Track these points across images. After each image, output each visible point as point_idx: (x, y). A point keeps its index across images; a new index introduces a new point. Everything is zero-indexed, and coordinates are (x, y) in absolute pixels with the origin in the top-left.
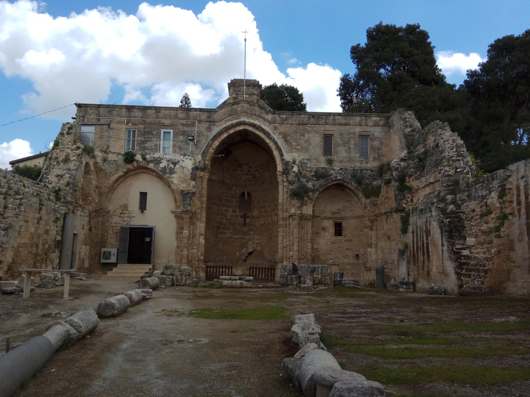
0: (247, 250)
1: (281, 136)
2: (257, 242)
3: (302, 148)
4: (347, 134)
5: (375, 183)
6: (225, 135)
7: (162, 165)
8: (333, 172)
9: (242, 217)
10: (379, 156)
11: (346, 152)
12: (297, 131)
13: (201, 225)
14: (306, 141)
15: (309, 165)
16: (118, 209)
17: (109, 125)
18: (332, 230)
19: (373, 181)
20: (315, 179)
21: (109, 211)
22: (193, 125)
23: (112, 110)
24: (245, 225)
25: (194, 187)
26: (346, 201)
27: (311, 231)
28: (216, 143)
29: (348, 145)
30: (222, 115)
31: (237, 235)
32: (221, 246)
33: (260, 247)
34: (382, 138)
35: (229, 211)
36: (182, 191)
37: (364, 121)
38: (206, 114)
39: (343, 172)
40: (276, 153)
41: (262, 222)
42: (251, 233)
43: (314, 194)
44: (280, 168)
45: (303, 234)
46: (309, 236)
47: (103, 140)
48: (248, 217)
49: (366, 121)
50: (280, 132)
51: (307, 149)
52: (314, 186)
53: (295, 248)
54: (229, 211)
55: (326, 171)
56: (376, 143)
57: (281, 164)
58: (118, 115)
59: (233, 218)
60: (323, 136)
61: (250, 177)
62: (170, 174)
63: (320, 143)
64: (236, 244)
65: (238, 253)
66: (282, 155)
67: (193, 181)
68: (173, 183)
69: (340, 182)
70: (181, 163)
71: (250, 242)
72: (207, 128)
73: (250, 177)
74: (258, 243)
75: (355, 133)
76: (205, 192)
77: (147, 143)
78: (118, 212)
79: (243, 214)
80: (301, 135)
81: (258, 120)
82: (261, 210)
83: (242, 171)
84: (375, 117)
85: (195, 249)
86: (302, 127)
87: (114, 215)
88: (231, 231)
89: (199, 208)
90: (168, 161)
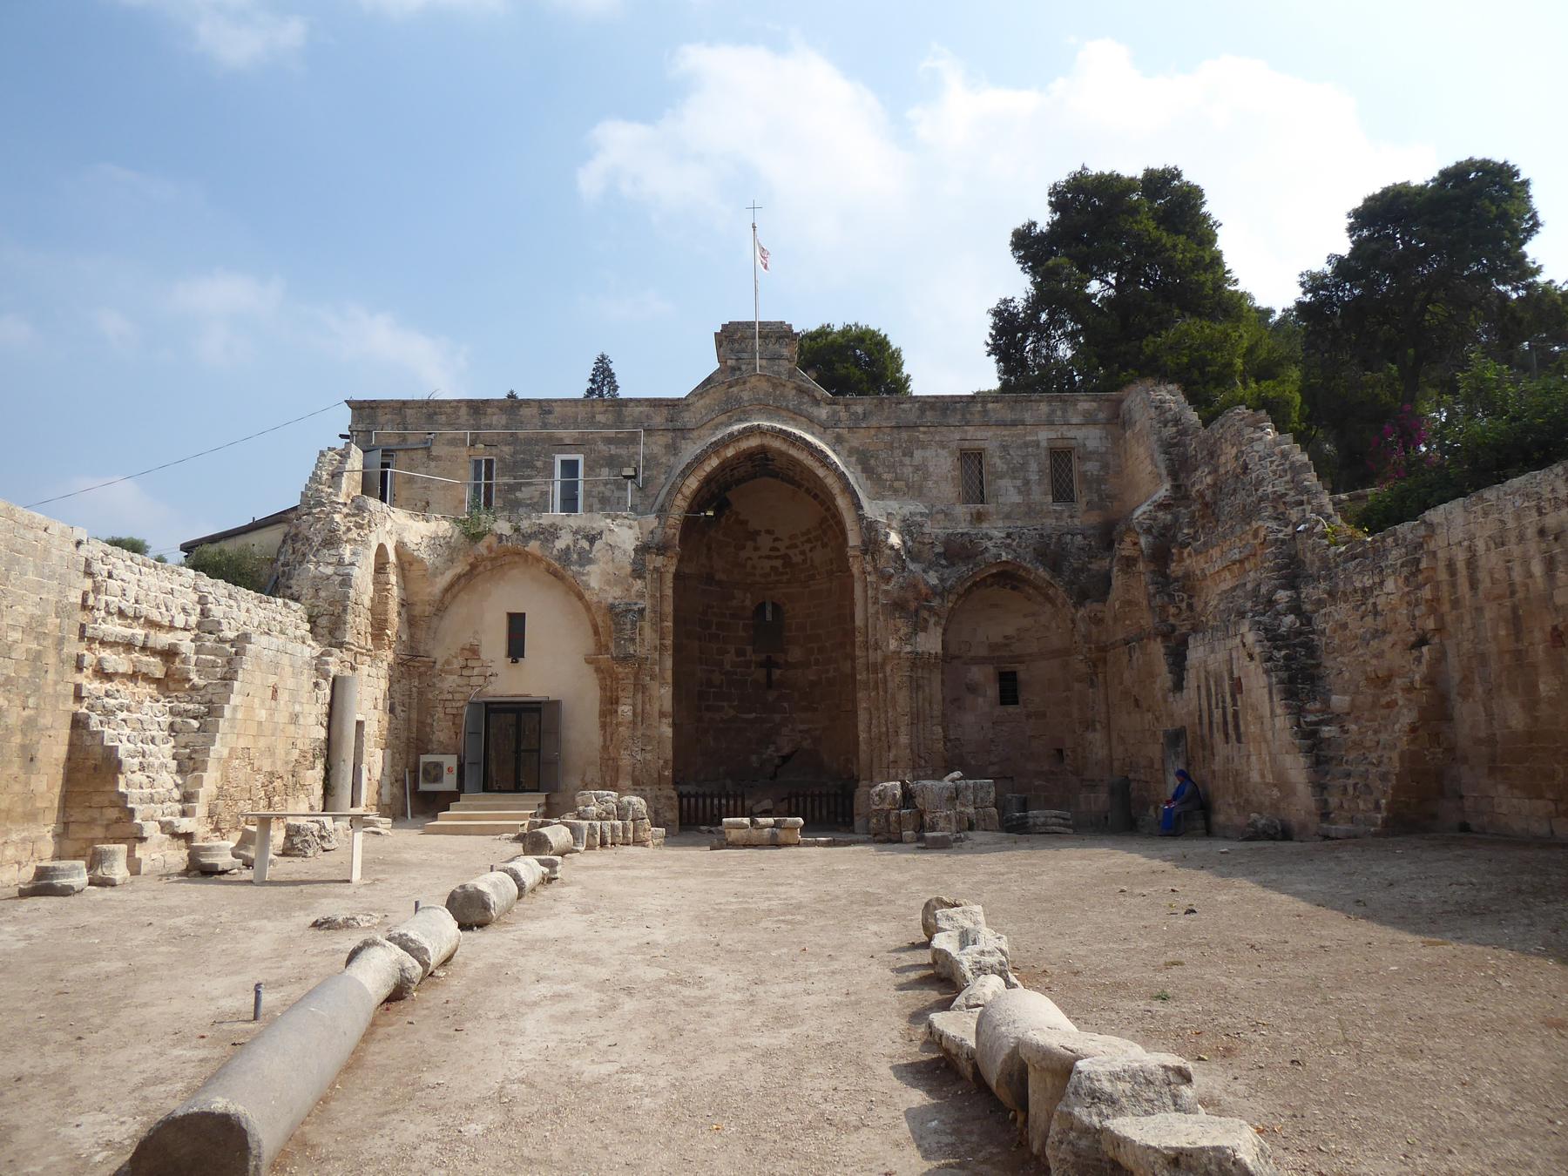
0: (777, 750)
1: (853, 459)
2: (802, 727)
3: (907, 486)
4: (1019, 447)
5: (1094, 567)
6: (715, 462)
7: (560, 544)
8: (989, 544)
9: (761, 665)
10: (1101, 499)
11: (1020, 492)
12: (892, 443)
13: (662, 691)
14: (917, 469)
15: (926, 530)
16: (456, 657)
17: (428, 449)
18: (993, 691)
19: (1091, 563)
20: (943, 562)
21: (435, 662)
22: (633, 439)
23: (435, 414)
24: (769, 684)
25: (641, 595)
26: (1025, 616)
27: (940, 697)
28: (693, 483)
29: (1022, 474)
30: (704, 412)
33: (809, 741)
34: (1106, 453)
36: (612, 607)
37: (1059, 413)
38: (665, 411)
39: (1014, 543)
40: (842, 502)
42: (786, 705)
43: (943, 600)
44: (854, 539)
45: (920, 704)
46: (937, 710)
47: (414, 486)
48: (777, 665)
49: (1065, 411)
50: (851, 448)
51: (920, 488)
52: (942, 580)
53: (904, 739)
54: (728, 652)
55: (971, 541)
56: (1092, 467)
57: (856, 528)
58: (450, 425)
60: (958, 455)
61: (778, 563)
62: (581, 566)
63: (953, 473)
65: (754, 758)
66: (858, 506)
67: (639, 582)
68: (588, 587)
69: (1009, 568)
70: (606, 537)
72: (667, 446)
73: (778, 563)
75: (1037, 444)
76: (668, 608)
77: (520, 490)
78: (457, 664)
79: (763, 656)
80: (904, 455)
81: (794, 419)
83: (756, 549)
84: (1085, 401)
85: (650, 751)
86: (904, 435)
87: (446, 672)
88: (736, 703)
89: (656, 647)
90: (576, 533)
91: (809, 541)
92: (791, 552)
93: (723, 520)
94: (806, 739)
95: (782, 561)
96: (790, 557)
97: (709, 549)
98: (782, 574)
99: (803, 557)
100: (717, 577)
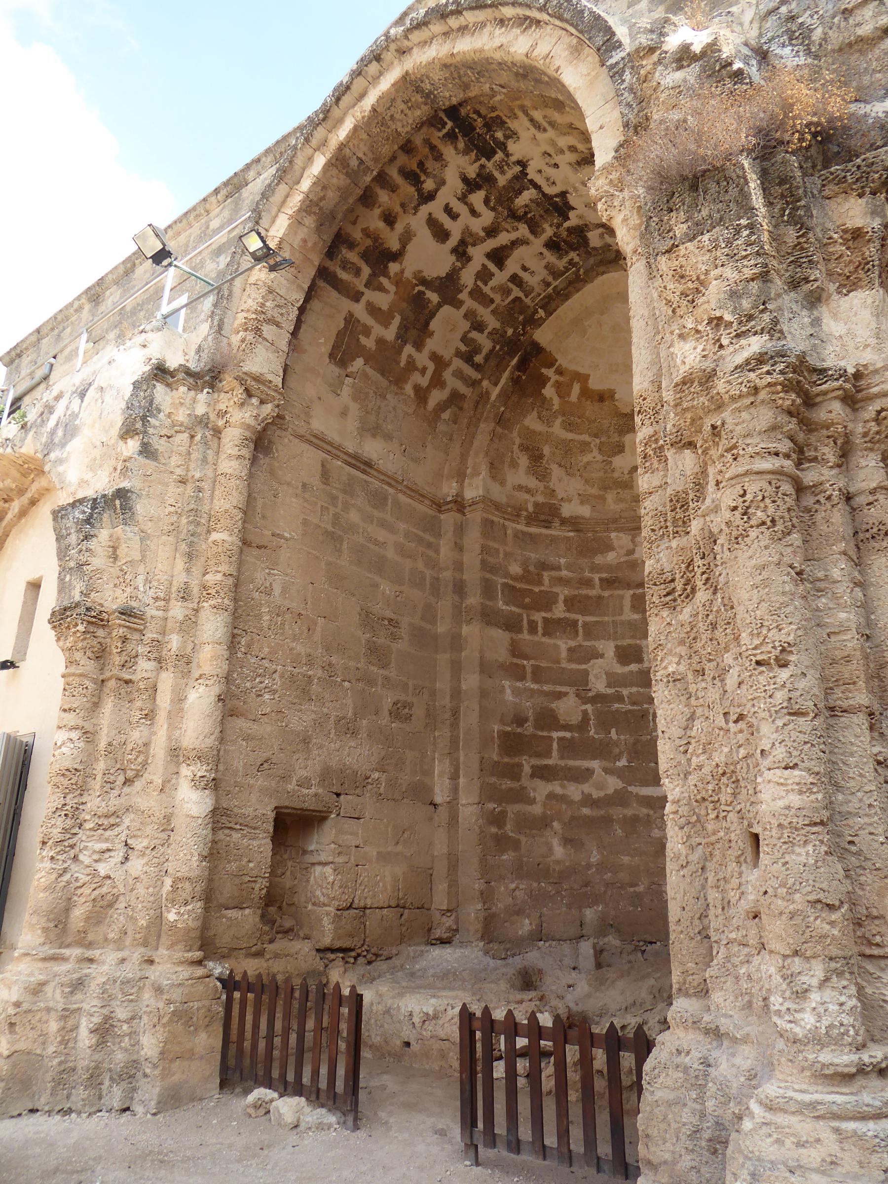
32: (559, 851)
54: (602, 656)
59: (625, 692)
88: (622, 763)
93: (549, 391)
97: (536, 457)
100: (567, 510)
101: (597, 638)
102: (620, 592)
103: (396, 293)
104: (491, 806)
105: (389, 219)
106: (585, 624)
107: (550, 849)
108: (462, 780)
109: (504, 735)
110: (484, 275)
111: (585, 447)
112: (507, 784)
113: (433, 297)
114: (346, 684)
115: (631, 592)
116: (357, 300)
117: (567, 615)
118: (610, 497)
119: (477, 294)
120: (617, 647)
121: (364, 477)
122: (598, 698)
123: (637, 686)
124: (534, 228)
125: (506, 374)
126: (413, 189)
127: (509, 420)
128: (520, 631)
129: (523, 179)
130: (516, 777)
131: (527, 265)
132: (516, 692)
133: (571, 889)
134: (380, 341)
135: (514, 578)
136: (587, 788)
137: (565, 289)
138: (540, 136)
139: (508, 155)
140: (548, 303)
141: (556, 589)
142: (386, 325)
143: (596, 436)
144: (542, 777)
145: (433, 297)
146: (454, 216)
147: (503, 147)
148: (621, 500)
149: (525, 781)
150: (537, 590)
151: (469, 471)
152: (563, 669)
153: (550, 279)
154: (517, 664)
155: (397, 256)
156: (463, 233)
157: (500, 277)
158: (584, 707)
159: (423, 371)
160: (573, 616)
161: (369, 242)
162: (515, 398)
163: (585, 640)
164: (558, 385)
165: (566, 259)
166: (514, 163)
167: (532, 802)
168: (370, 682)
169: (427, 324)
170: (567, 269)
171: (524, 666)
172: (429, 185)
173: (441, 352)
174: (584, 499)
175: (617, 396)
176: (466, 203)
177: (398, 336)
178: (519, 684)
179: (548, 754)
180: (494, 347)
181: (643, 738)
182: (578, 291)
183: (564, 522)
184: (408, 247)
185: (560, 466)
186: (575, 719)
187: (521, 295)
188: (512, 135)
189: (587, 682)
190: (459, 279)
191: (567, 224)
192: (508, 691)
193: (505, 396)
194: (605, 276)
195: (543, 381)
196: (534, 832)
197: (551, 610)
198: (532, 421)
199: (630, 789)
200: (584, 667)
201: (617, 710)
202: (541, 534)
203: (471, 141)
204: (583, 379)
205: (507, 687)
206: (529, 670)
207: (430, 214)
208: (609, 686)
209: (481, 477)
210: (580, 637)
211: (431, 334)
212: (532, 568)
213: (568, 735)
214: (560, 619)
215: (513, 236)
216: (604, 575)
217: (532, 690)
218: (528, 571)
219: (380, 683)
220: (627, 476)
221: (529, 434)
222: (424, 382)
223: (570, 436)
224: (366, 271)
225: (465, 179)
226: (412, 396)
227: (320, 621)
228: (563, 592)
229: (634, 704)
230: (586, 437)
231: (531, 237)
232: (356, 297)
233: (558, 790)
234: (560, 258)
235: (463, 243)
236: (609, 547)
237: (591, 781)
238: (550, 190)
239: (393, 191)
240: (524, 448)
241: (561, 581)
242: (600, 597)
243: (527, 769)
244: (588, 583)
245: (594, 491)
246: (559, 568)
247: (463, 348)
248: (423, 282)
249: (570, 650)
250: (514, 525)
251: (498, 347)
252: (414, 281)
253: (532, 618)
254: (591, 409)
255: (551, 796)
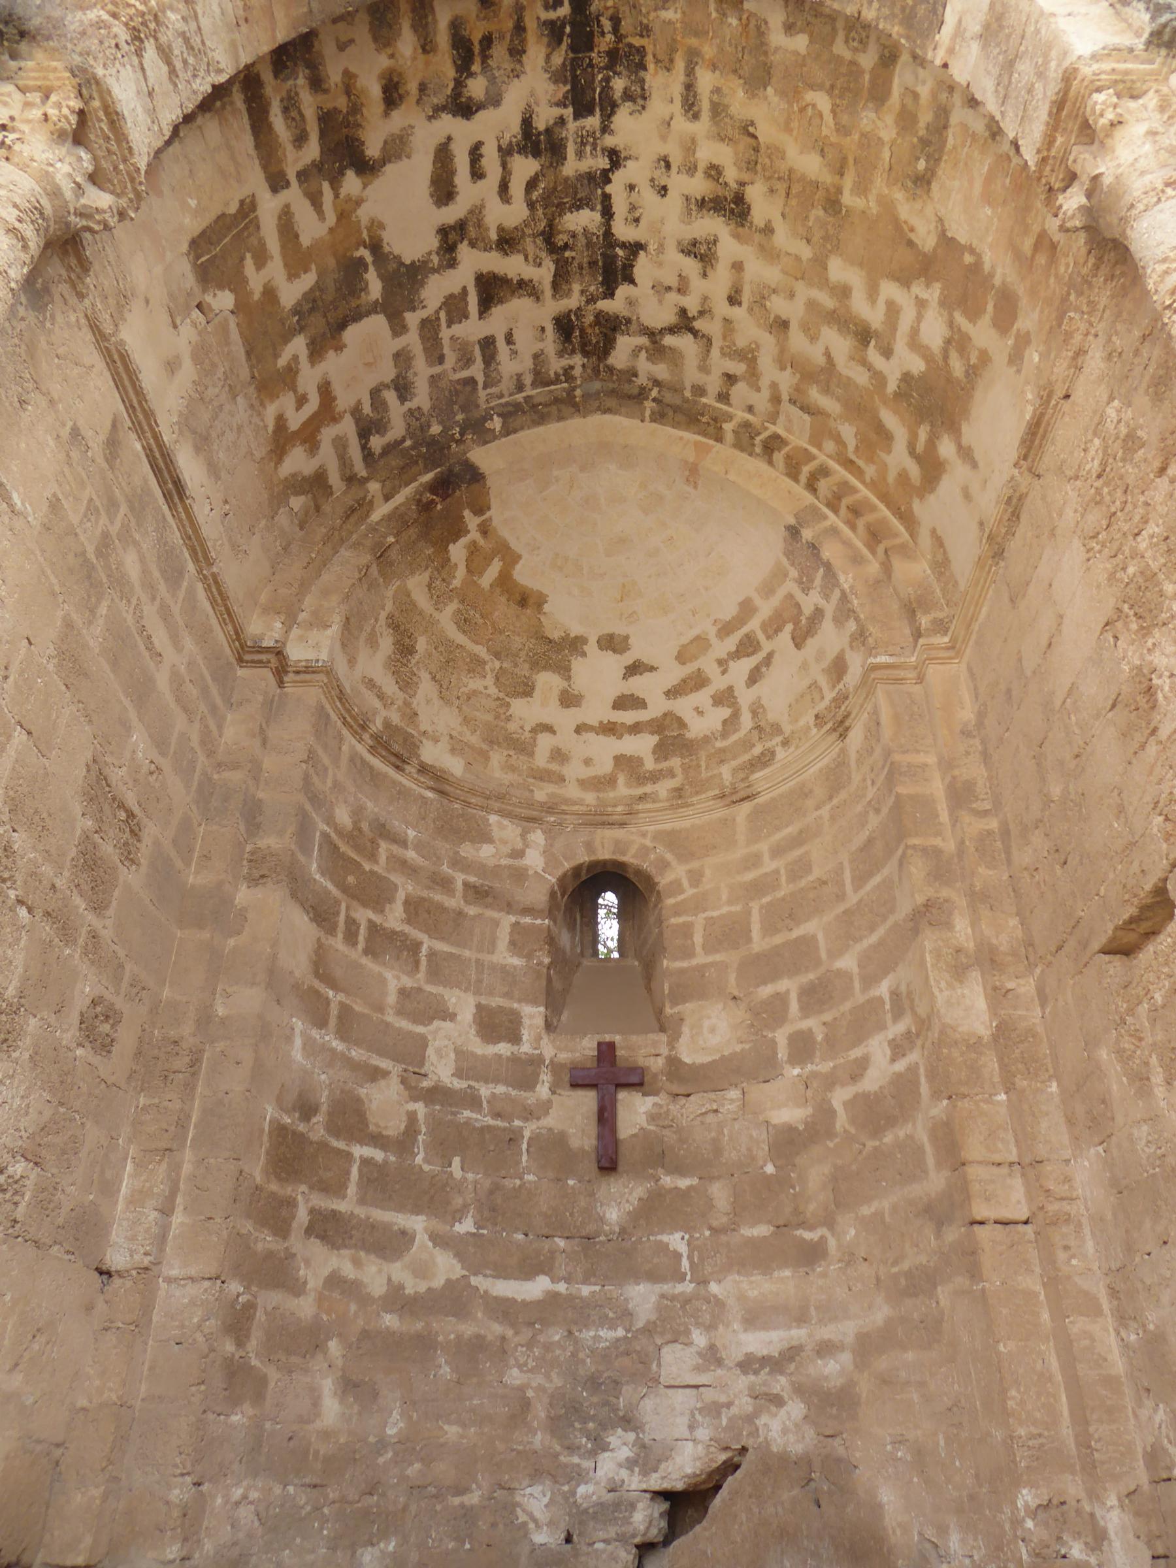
31: (528, 1270)
32: (331, 1408)
33: (795, 1409)
35: (452, 1017)
41: (790, 1115)
42: (677, 1241)
48: (637, 1081)
54: (452, 1017)
59: (485, 1091)
61: (642, 746)
64: (515, 1377)
71: (671, 1354)
73: (642, 746)
74: (775, 1364)
79: (587, 1047)
82: (766, 991)
88: (466, 1226)
91: (748, 646)
92: (684, 706)
94: (777, 1401)
95: (655, 739)
96: (682, 724)
97: (405, 649)
98: (654, 777)
99: (725, 712)
100: (430, 753)
101: (447, 983)
102: (495, 915)
103: (331, 230)
104: (235, 1287)
105: (392, 95)
106: (432, 954)
107: (316, 1403)
108: (178, 1219)
109: (280, 1132)
110: (455, 307)
111: (476, 666)
112: (266, 1241)
113: (375, 286)
114: (23, 912)
115: (512, 919)
116: (275, 189)
117: (407, 929)
118: (497, 757)
119: (429, 328)
120: (479, 1007)
121: (165, 508)
122: (436, 1095)
123: (507, 1083)
124: (560, 282)
125: (407, 492)
126: (451, 73)
127: (391, 564)
128: (331, 931)
129: (597, 185)
130: (282, 1229)
131: (516, 336)
132: (310, 1047)
133: (343, 1500)
134: (270, 293)
135: (340, 832)
136: (398, 1271)
137: (546, 405)
138: (682, 125)
139: (605, 129)
140: (510, 414)
141: (396, 878)
142: (292, 276)
143: (497, 655)
144: (323, 1237)
145: (375, 286)
146: (477, 174)
147: (609, 108)
148: (513, 769)
149: (296, 1242)
150: (367, 867)
151: (302, 616)
152: (388, 1024)
153: (528, 380)
154: (317, 993)
155: (366, 168)
156: (471, 212)
157: (472, 329)
158: (412, 1106)
159: (301, 401)
160: (417, 934)
161: (342, 103)
162: (413, 532)
163: (428, 982)
164: (473, 549)
165: (565, 362)
166: (603, 150)
167: (297, 1289)
168: (67, 932)
169: (342, 326)
170: (557, 381)
171: (327, 1001)
172: (476, 87)
173: (338, 390)
174: (457, 747)
175: (547, 608)
176: (504, 165)
177: (296, 311)
178: (315, 1033)
179: (336, 1188)
180: (403, 440)
181: (508, 1183)
182: (561, 418)
183: (424, 769)
184: (389, 168)
185: (434, 678)
186: (394, 1127)
187: (480, 379)
188: (638, 97)
189: (422, 1062)
190: (422, 284)
191: (604, 305)
192: (298, 1042)
193: (398, 520)
194: (608, 417)
195: (457, 531)
196: (294, 1359)
197: (382, 912)
198: (417, 585)
199: (475, 1281)
200: (420, 1029)
201: (467, 1123)
202: (385, 776)
203: (574, 64)
204: (511, 558)
205: (297, 1031)
206: (334, 1010)
207: (449, 138)
208: (459, 1074)
209: (329, 632)
210: (421, 975)
211: (340, 348)
212: (365, 826)
213: (378, 1155)
214: (394, 932)
215: (528, 272)
216: (472, 879)
217: (333, 1051)
218: (360, 830)
219: (81, 941)
220: (527, 735)
221: (406, 605)
222: (295, 421)
223: (461, 639)
224: (313, 150)
225: (527, 122)
226: (270, 429)
227: (19, 736)
228: (405, 887)
229: (498, 1115)
230: (481, 651)
231: (548, 292)
232: (277, 183)
233: (348, 1270)
234: (560, 354)
235: (461, 227)
236: (484, 837)
237: (407, 1259)
238: (622, 231)
239: (425, 51)
240: (394, 625)
241: (404, 865)
242: (460, 914)
243: (302, 1215)
244: (445, 884)
245: (474, 739)
246: (404, 844)
247: (367, 409)
248: (376, 247)
249: (403, 993)
250: (354, 741)
251: (408, 443)
252: (365, 235)
253: (353, 914)
254: (503, 609)
255: (335, 1281)
